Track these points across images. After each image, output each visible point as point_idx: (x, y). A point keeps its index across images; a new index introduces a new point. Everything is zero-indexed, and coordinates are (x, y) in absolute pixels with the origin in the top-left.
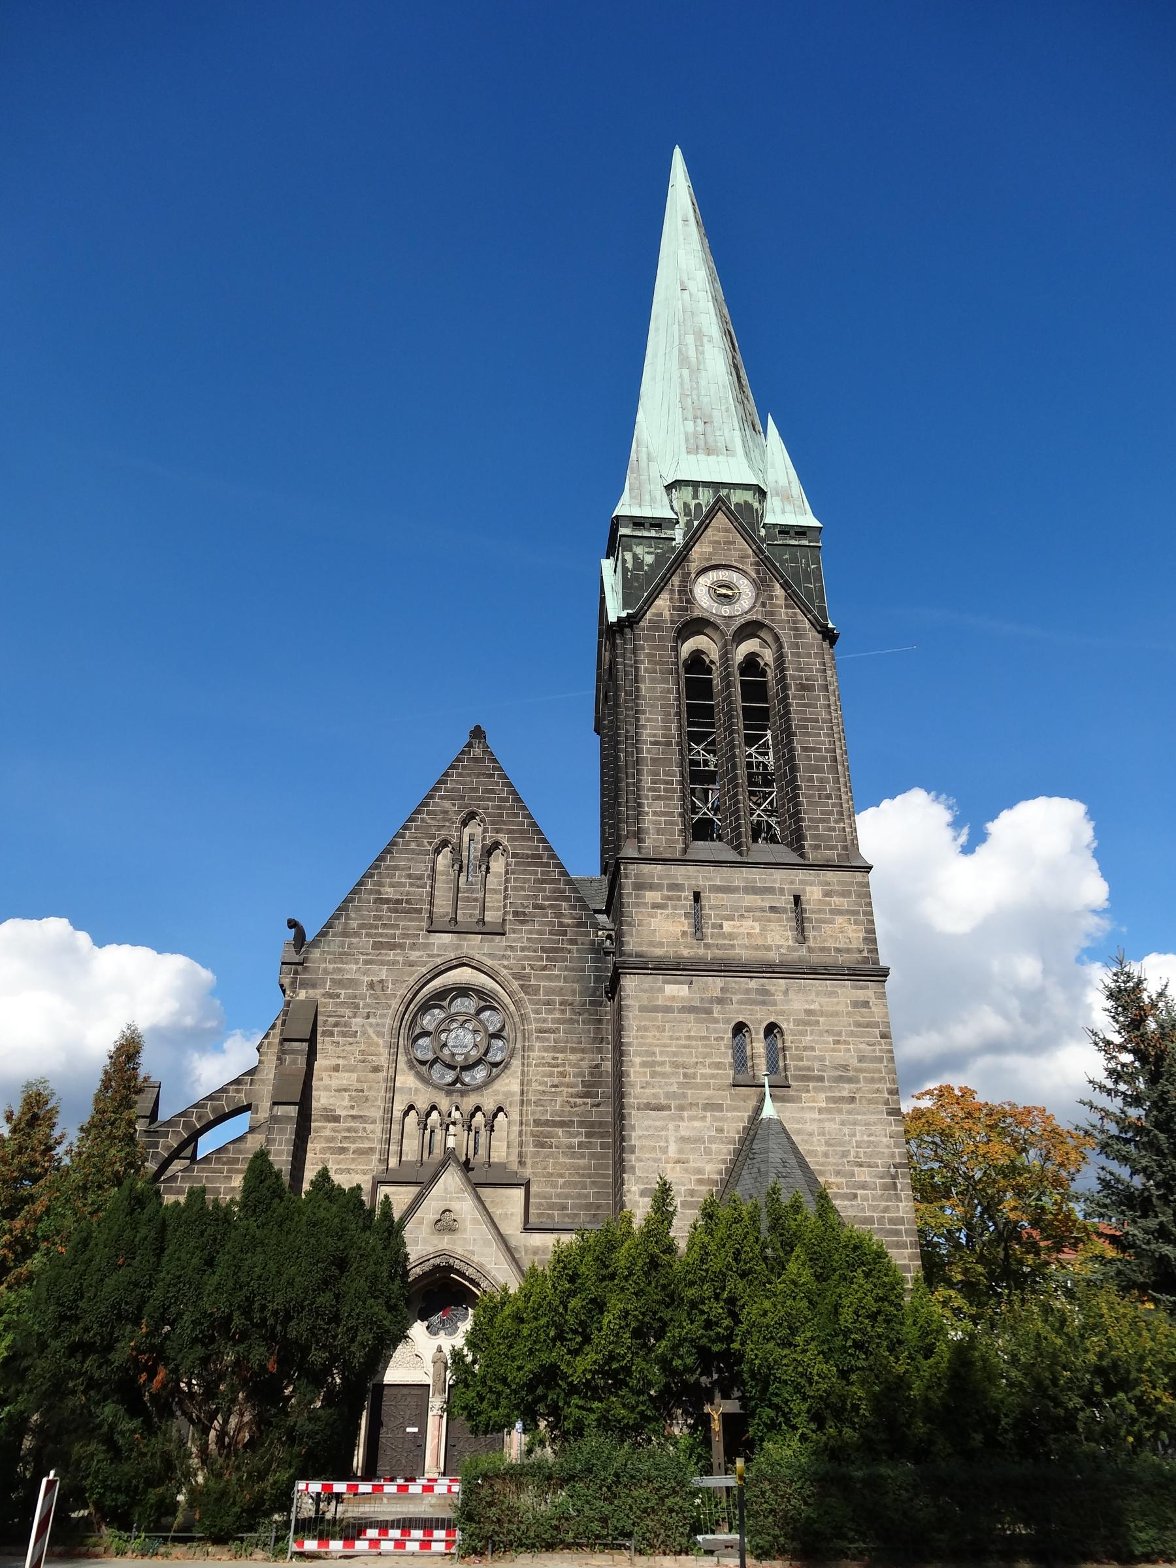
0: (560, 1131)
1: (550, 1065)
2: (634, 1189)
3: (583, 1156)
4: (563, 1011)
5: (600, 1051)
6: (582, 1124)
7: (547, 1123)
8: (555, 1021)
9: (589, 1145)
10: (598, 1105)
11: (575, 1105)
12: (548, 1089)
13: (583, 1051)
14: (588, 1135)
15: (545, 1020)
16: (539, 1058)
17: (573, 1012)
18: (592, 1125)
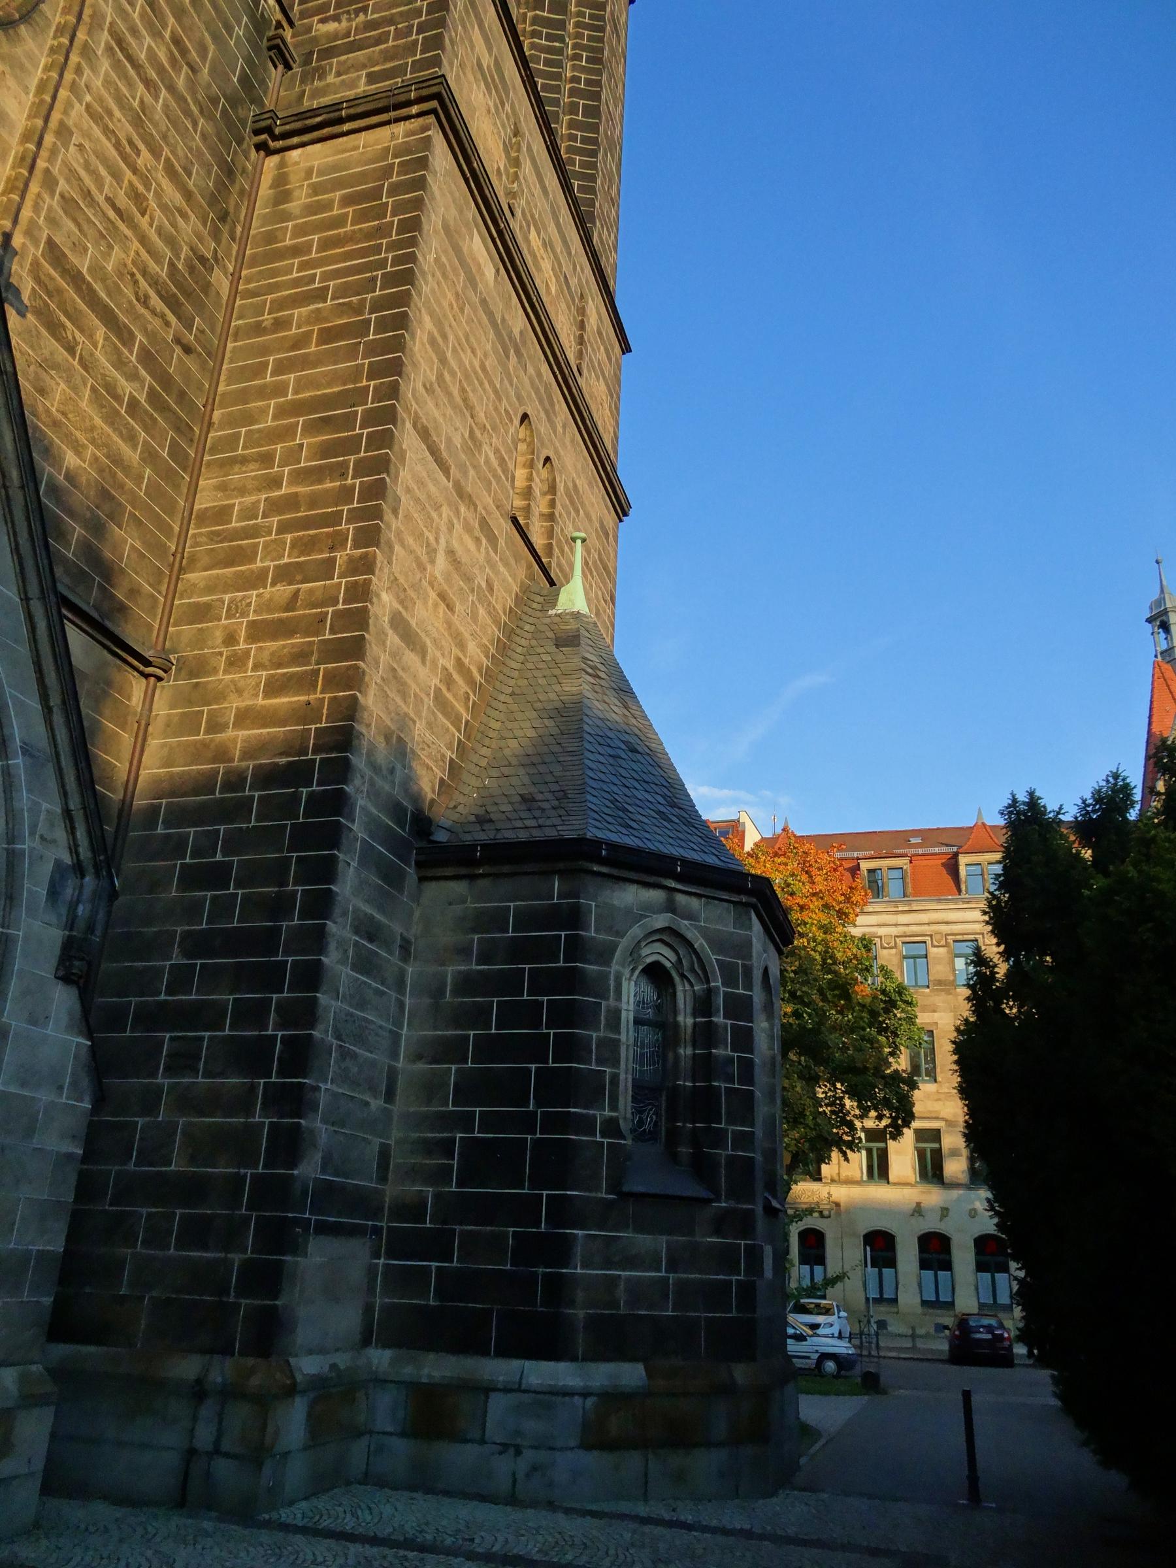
0: (101, 332)
1: (118, 146)
2: (385, 597)
3: (131, 439)
4: (173, 61)
5: (216, 235)
6: (147, 358)
7: (76, 278)
8: (152, 56)
9: (149, 426)
10: (188, 350)
11: (145, 301)
12: (101, 199)
13: (188, 195)
14: (152, 396)
15: (134, 31)
16: (100, 100)
17: (192, 85)
18: (165, 380)
